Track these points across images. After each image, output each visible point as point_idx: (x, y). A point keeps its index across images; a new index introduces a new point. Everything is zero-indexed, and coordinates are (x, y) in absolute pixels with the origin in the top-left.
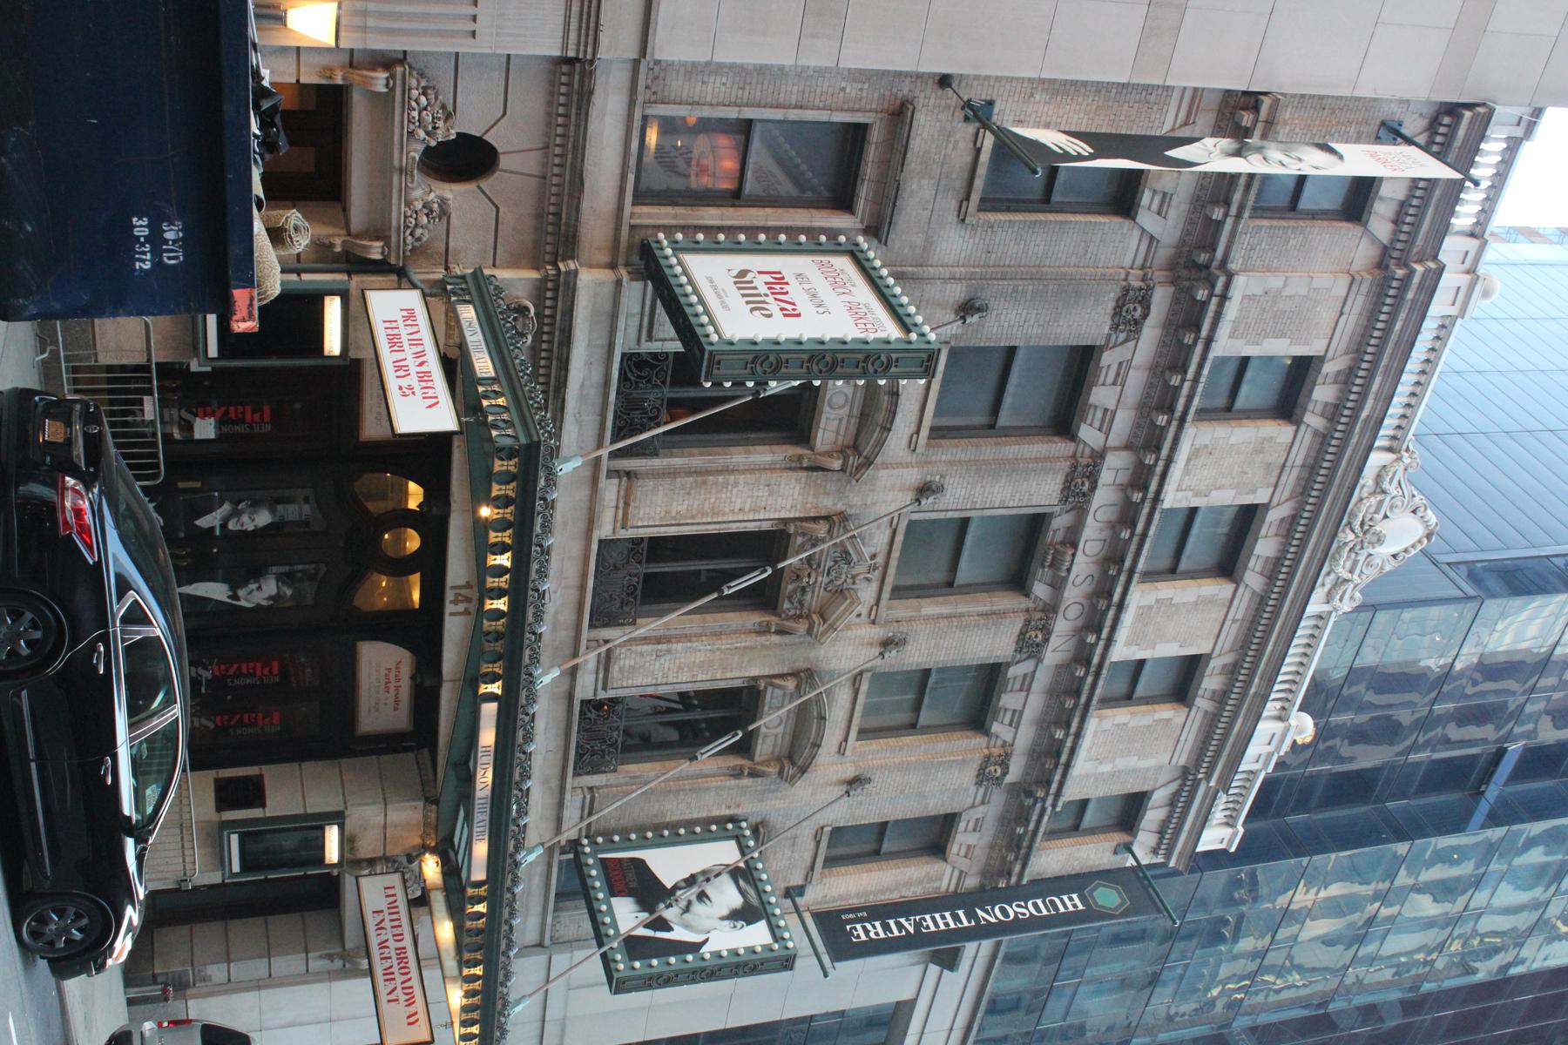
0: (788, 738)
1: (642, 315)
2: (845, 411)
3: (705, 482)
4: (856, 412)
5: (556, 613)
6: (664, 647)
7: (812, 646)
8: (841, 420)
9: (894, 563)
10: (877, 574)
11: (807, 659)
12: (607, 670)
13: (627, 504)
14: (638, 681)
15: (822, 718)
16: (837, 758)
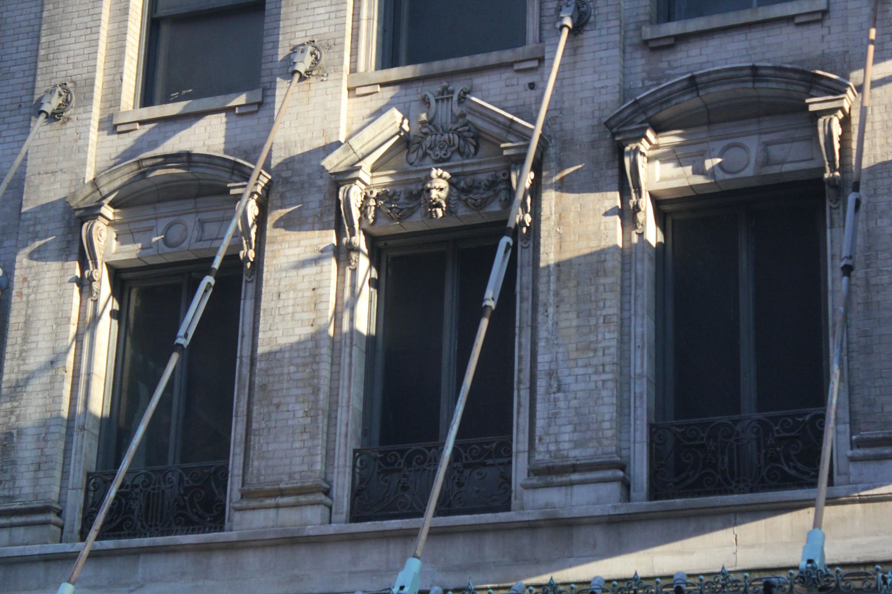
0: (767, 123)
1: (12, 526)
2: (190, 221)
3: (263, 387)
4: (189, 205)
5: (447, 570)
6: (541, 384)
7: (566, 144)
8: (202, 223)
9: (436, 66)
10: (458, 87)
11: (593, 144)
12: (574, 468)
13: (282, 493)
14: (607, 411)
15: (693, 84)
16: (833, 21)
